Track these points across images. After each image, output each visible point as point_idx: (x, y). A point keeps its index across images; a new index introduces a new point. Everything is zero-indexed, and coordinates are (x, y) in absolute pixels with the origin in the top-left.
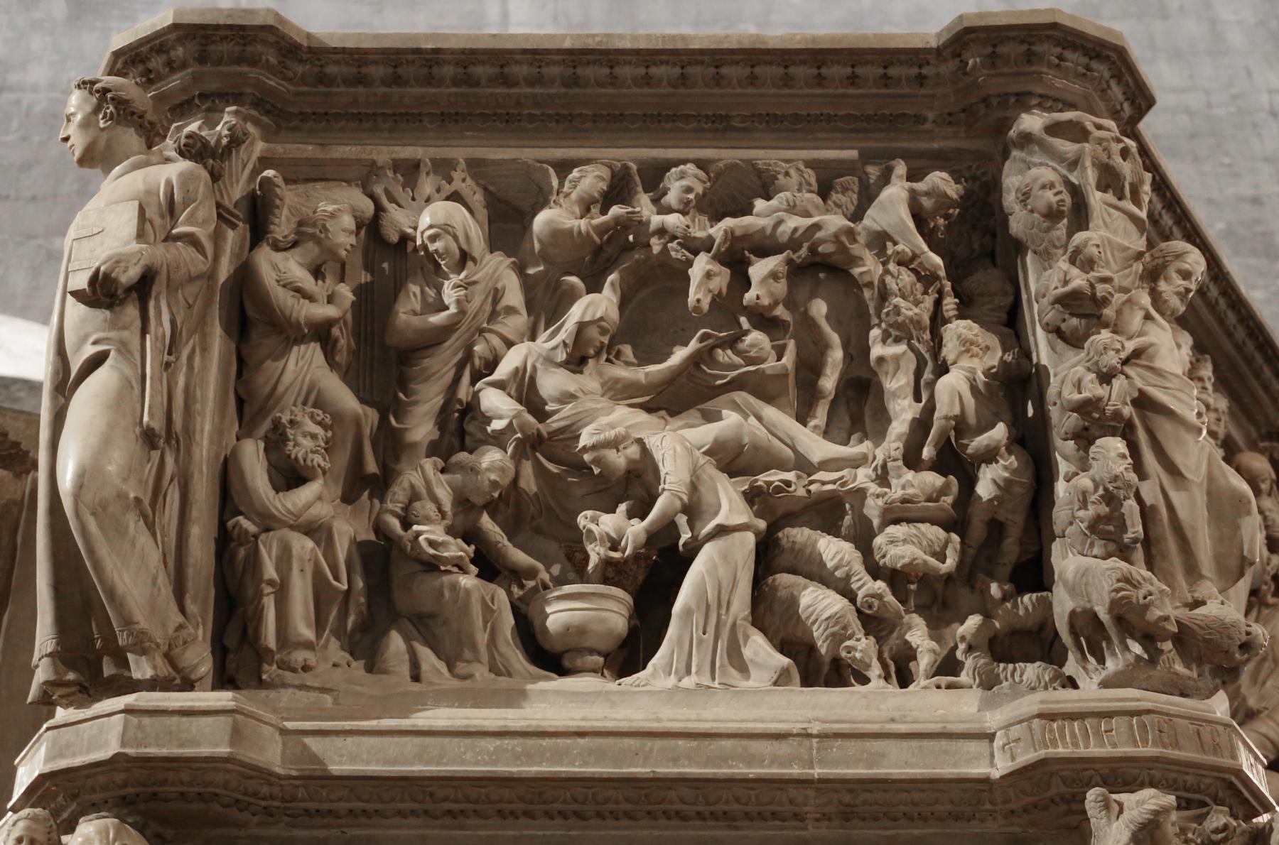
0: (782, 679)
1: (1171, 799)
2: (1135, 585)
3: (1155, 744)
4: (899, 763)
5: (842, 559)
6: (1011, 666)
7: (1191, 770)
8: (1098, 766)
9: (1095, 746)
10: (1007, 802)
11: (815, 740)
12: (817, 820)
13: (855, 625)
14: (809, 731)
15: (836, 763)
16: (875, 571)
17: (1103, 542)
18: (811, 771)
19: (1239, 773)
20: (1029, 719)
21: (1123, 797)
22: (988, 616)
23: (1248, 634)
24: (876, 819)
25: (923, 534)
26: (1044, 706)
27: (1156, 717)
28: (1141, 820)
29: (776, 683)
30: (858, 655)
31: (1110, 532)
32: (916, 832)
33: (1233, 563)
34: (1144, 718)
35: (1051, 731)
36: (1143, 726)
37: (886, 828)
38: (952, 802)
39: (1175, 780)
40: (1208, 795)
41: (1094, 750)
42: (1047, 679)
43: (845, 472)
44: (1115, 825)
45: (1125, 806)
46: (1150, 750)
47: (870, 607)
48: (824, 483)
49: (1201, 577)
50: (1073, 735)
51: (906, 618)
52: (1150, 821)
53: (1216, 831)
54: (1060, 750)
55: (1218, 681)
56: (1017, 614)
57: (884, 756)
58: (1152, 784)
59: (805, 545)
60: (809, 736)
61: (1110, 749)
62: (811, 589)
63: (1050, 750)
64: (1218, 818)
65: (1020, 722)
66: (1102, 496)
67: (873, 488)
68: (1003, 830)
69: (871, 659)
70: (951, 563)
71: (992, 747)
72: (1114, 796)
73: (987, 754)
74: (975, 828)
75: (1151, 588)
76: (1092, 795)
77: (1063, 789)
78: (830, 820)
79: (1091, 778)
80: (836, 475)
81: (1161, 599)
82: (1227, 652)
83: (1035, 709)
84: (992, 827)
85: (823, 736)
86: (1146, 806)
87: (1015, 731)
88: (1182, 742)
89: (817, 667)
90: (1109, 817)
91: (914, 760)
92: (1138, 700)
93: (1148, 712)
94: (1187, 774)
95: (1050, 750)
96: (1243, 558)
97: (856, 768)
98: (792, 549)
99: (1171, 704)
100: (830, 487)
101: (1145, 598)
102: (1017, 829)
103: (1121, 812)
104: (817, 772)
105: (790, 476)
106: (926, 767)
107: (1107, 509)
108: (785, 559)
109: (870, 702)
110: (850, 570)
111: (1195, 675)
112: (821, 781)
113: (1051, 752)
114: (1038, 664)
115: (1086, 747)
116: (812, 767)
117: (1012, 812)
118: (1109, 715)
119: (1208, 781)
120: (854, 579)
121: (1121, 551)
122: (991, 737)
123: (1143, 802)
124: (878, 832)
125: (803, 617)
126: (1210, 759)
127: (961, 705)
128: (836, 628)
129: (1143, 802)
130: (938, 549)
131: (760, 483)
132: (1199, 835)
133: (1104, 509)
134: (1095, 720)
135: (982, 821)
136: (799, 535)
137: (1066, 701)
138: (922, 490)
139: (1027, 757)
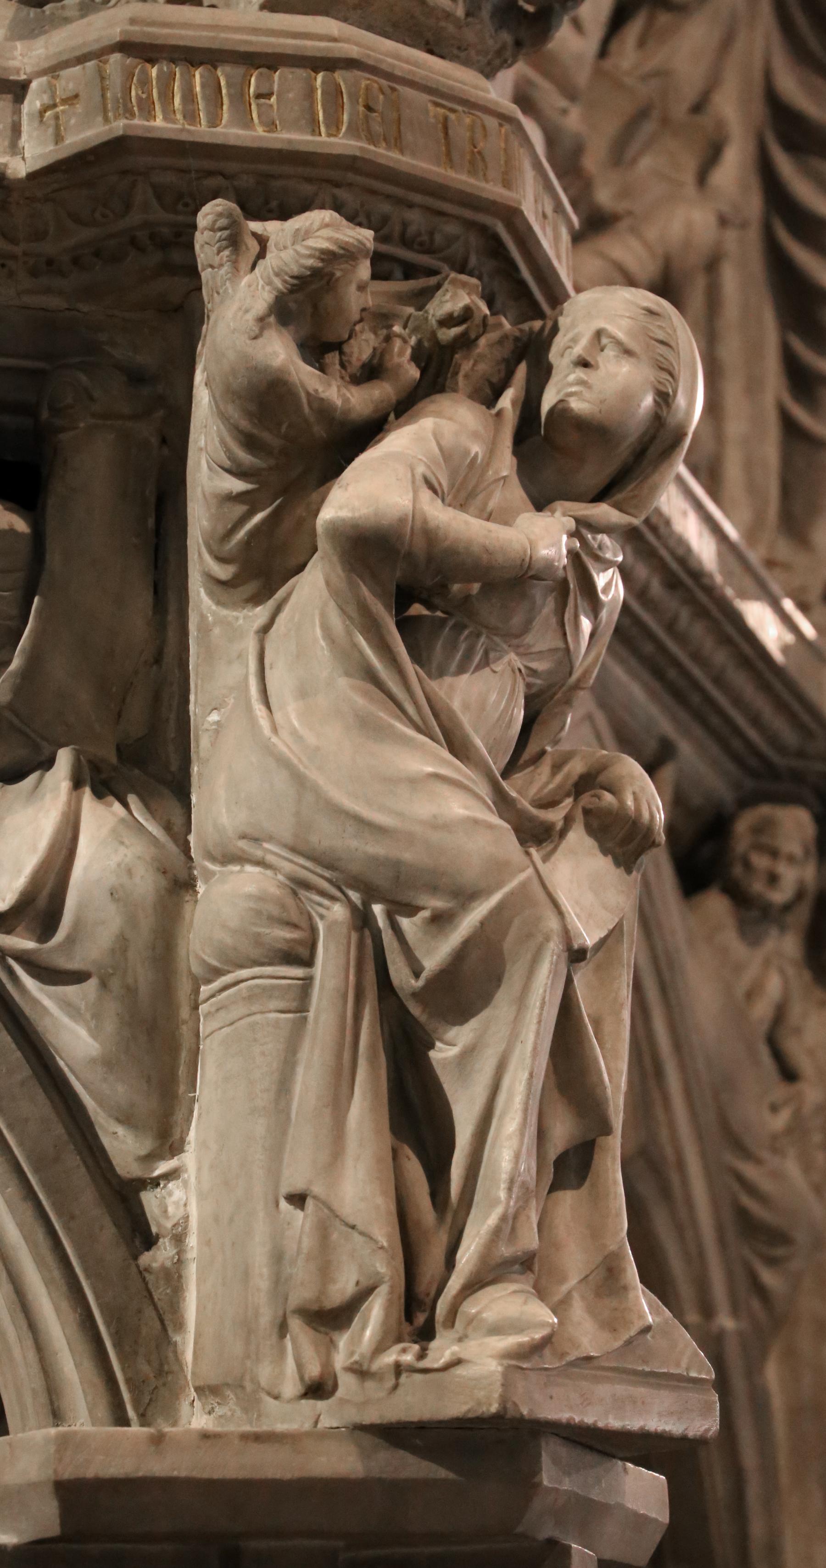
3: (353, 131)
7: (418, 198)
8: (231, 167)
9: (231, 124)
10: (39, 236)
19: (512, 216)
20: (101, 54)
26: (136, 28)
27: (364, 80)
28: (295, 270)
34: (339, 76)
35: (145, 82)
36: (334, 95)
41: (229, 131)
44: (246, 280)
45: (271, 244)
46: (342, 143)
50: (189, 96)
52: (316, 273)
53: (448, 321)
54: (159, 122)
61: (260, 131)
63: (136, 121)
64: (456, 297)
65: (81, 60)
68: (27, 300)
71: (18, 112)
72: (255, 226)
76: (209, 214)
77: (159, 214)
83: (115, 34)
86: (311, 243)
87: (72, 79)
88: (408, 137)
90: (235, 265)
92: (335, 40)
93: (351, 64)
94: (411, 206)
99: (398, 57)
102: (55, 302)
103: (262, 254)
113: (138, 124)
115: (214, 121)
117: (50, 262)
118: (270, 61)
119: (452, 228)
126: (459, 178)
129: (307, 234)
132: (415, 330)
134: (240, 70)
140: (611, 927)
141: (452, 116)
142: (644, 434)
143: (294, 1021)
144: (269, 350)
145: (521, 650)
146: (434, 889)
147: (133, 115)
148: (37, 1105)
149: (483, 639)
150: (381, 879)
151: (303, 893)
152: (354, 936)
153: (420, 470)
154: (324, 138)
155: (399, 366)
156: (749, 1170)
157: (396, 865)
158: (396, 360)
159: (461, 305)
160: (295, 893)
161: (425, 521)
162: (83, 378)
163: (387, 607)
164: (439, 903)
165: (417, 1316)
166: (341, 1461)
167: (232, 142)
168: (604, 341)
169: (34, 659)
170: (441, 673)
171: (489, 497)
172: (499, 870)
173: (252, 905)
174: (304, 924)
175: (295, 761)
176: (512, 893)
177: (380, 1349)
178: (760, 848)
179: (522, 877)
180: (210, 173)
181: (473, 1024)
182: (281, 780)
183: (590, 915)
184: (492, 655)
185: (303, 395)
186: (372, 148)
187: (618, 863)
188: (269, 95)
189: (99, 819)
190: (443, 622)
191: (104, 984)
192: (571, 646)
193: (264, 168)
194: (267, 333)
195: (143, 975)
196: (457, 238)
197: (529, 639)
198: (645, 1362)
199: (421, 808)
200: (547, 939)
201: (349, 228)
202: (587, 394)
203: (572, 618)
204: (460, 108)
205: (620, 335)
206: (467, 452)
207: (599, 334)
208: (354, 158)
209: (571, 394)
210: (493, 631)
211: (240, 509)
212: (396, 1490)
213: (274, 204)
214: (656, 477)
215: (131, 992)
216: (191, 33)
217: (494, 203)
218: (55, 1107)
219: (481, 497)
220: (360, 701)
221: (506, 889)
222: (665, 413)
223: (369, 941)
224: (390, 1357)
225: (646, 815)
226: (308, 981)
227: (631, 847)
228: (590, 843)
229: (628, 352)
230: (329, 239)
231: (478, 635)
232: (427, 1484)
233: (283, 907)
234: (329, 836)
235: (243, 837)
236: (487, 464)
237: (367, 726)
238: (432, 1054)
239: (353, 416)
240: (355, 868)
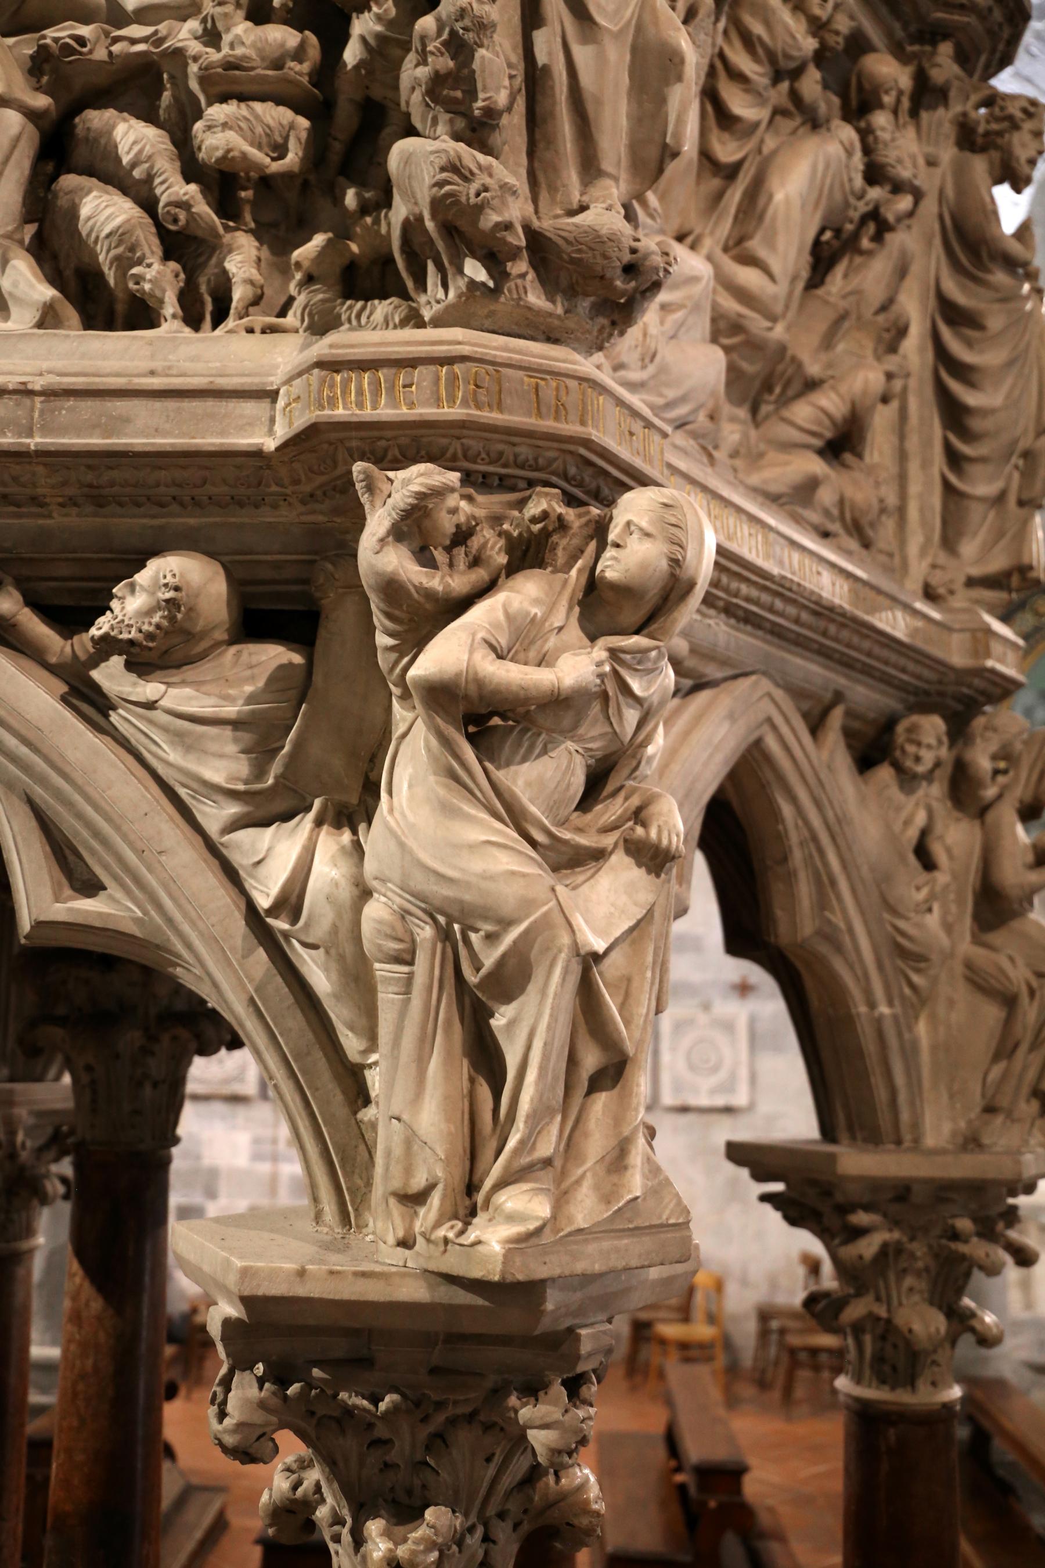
0: (48, 318)
1: (454, 477)
2: (467, 177)
3: (465, 403)
4: (148, 430)
5: (141, 151)
6: (360, 304)
9: (386, 406)
10: (296, 482)
11: (38, 400)
12: (62, 505)
13: (150, 245)
14: (30, 387)
15: (63, 431)
16: (192, 168)
17: (448, 116)
18: (28, 441)
20: (308, 370)
21: (391, 474)
22: (342, 234)
23: (634, 251)
24: (138, 505)
25: (257, 117)
28: (402, 506)
29: (40, 325)
30: (147, 287)
31: (455, 101)
32: (192, 521)
33: (652, 153)
34: (457, 368)
35: (332, 386)
36: (453, 379)
37: (153, 517)
38: (224, 481)
39: (501, 454)
40: (553, 473)
41: (385, 412)
42: (397, 320)
43: (163, 28)
47: (175, 221)
48: (134, 41)
49: (600, 173)
50: (360, 392)
51: (227, 238)
53: (534, 520)
55: (603, 321)
56: (378, 232)
57: (127, 420)
58: (430, 459)
59: (100, 134)
60: (31, 393)
61: (405, 410)
62: (94, 193)
63: (327, 412)
65: (300, 374)
66: (445, 44)
67: (195, 47)
69: (164, 291)
70: (293, 158)
71: (273, 409)
73: (265, 419)
74: (267, 516)
75: (488, 181)
78: (76, 505)
79: (386, 450)
80: (150, 30)
81: (502, 198)
82: (602, 277)
84: (288, 516)
85: (51, 394)
88: (507, 401)
89: (95, 299)
91: (167, 426)
93: (463, 359)
95: (327, 412)
96: (665, 146)
97: (91, 436)
98: (87, 139)
100: (141, 47)
101: (478, 195)
102: (321, 518)
104: (35, 442)
105: (85, 31)
106: (183, 435)
107: (451, 64)
108: (81, 155)
109: (172, 350)
110: (152, 167)
111: (560, 310)
112: (43, 454)
114: (392, 299)
115: (374, 408)
116: (30, 435)
118: (411, 363)
119: (551, 454)
120: (157, 181)
121: (474, 130)
122: (273, 395)
123: (414, 479)
124: (145, 521)
125: (84, 233)
127: (276, 356)
128: (120, 250)
130: (280, 140)
131: (48, 41)
132: (517, 526)
133: (446, 63)
134: (393, 371)
135: (275, 506)
136: (95, 118)
137: (364, 345)
138: (260, 51)
139: (301, 422)
140: (639, 917)
141: (542, 383)
142: (664, 588)
143: (403, 1000)
144: (386, 560)
146: (486, 918)
147: (323, 408)
148: (296, 1021)
149: (543, 736)
150: (454, 912)
151: (408, 917)
152: (439, 946)
153: (481, 635)
154: (446, 410)
155: (490, 557)
156: (902, 924)
157: (461, 902)
158: (488, 553)
159: (540, 509)
160: (403, 918)
161: (476, 673)
162: (329, 566)
163: (458, 729)
164: (489, 927)
165: (468, 1200)
166: (415, 1291)
167: (384, 419)
168: (633, 528)
169: (298, 745)
170: (508, 764)
171: (546, 641)
172: (528, 904)
173: (378, 926)
174: (407, 939)
175: (400, 833)
176: (535, 922)
177: (438, 1225)
178: (911, 741)
179: (545, 909)
180: (380, 438)
181: (514, 1005)
182: (393, 846)
183: (623, 912)
184: (549, 746)
186: (479, 413)
187: (649, 871)
188: (410, 386)
189: (330, 845)
190: (512, 728)
191: (327, 952)
193: (415, 432)
194: (385, 549)
195: (349, 949)
196: (556, 459)
197: (581, 731)
198: (630, 1221)
199: (477, 865)
200: (560, 951)
201: (439, 474)
202: (617, 567)
205: (644, 524)
206: (528, 613)
207: (628, 524)
208: (464, 421)
209: (607, 567)
210: (550, 731)
211: (394, 656)
212: (452, 1310)
213: (423, 453)
214: (675, 614)
215: (341, 958)
216: (362, 350)
217: (571, 437)
218: (308, 1021)
219: (539, 642)
220: (442, 792)
221: (532, 919)
223: (449, 950)
224: (441, 1232)
225: (665, 842)
226: (411, 974)
227: (659, 860)
228: (628, 861)
229: (648, 535)
230: (421, 484)
231: (539, 735)
232: (470, 1308)
233: (393, 928)
234: (421, 882)
235: (376, 878)
236: (545, 619)
237: (447, 810)
238: (492, 1022)
239: (454, 594)
240: (437, 902)
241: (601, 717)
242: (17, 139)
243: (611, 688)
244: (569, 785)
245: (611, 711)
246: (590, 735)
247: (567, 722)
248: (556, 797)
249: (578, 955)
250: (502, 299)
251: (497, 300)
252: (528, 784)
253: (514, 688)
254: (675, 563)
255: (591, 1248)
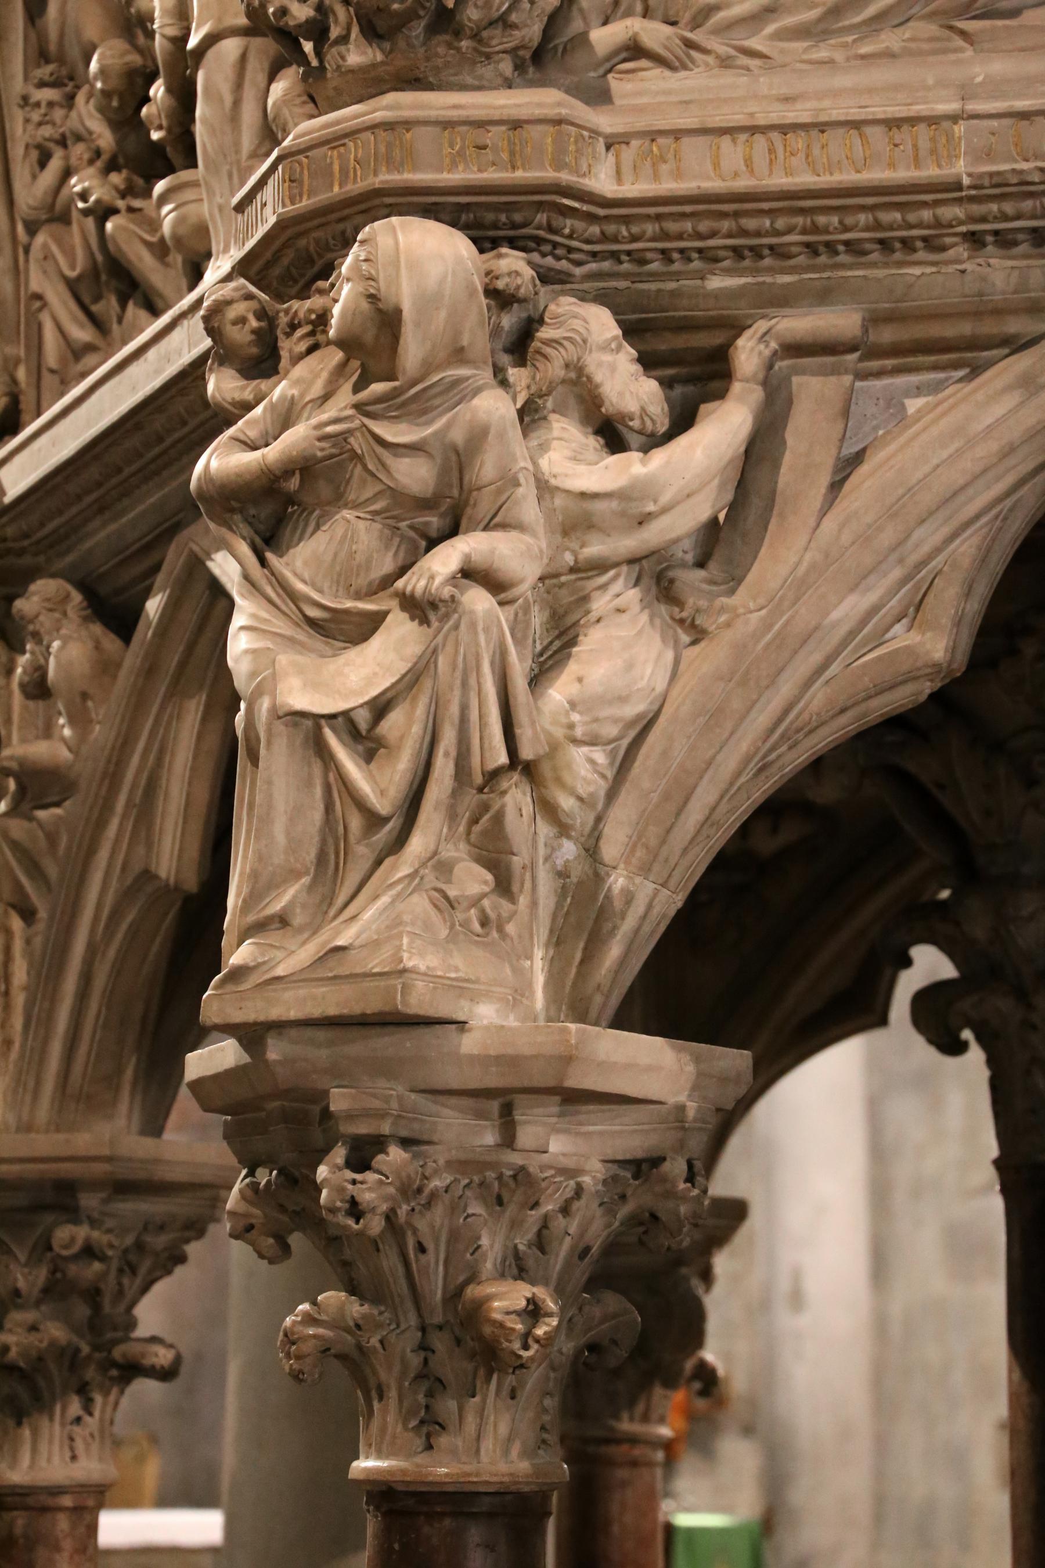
111: (380, 57)
140: (403, 672)
141: (342, 149)
145: (350, 505)
185: (229, 407)
192: (392, 485)
197: (352, 496)
198: (331, 971)
203: (380, 467)
204: (346, 141)
222: (381, 306)
231: (311, 513)
241: (369, 478)
242: (243, 58)
243: (357, 443)
244: (352, 555)
245: (370, 466)
246: (362, 499)
247: (324, 490)
248: (338, 568)
249: (279, 718)
250: (329, 75)
251: (325, 78)
252: (306, 563)
253: (233, 478)
254: (373, 298)
255: (288, 995)
